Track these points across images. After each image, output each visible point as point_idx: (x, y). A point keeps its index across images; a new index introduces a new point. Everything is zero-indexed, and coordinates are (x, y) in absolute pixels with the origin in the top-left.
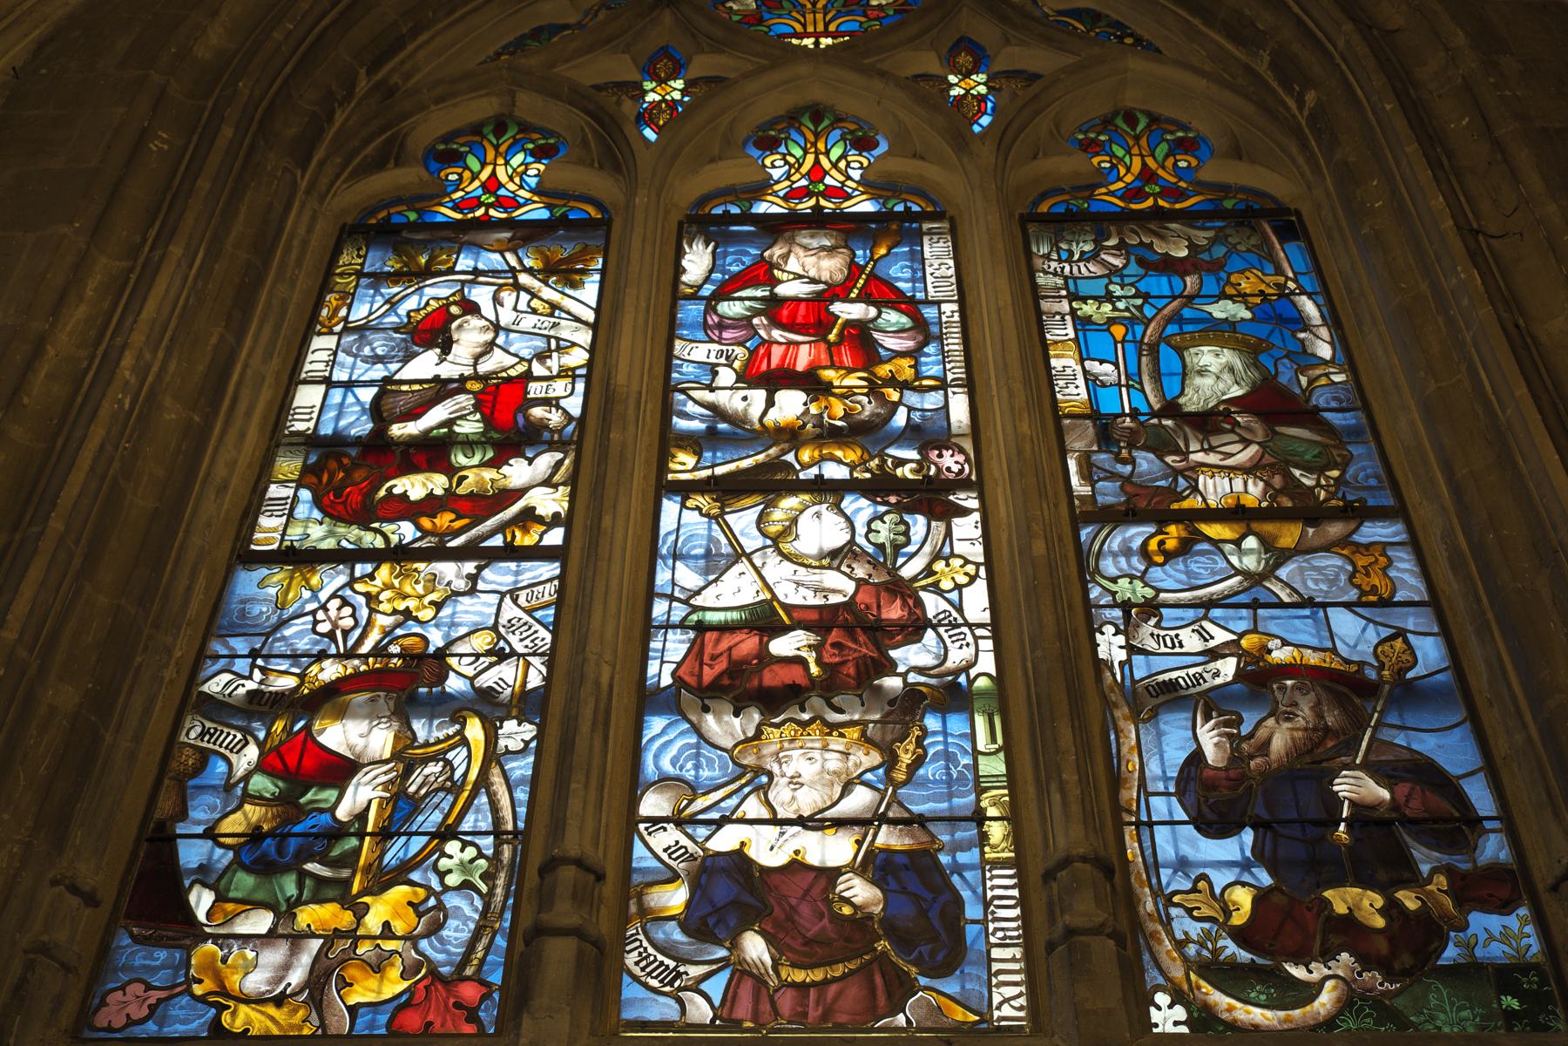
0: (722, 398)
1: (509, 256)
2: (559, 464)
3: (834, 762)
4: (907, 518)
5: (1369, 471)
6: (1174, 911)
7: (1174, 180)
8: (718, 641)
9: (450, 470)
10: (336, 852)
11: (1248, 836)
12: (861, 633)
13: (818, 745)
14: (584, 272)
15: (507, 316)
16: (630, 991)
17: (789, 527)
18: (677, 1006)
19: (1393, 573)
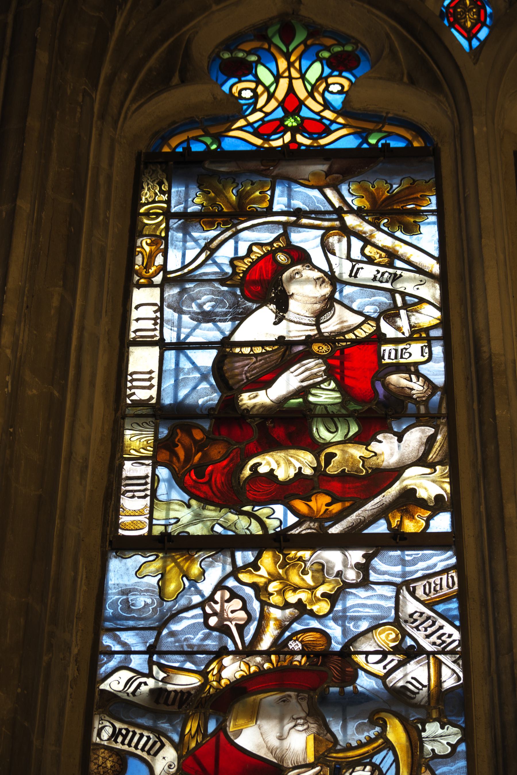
1: (329, 192)
2: (431, 441)
9: (315, 447)
14: (417, 213)
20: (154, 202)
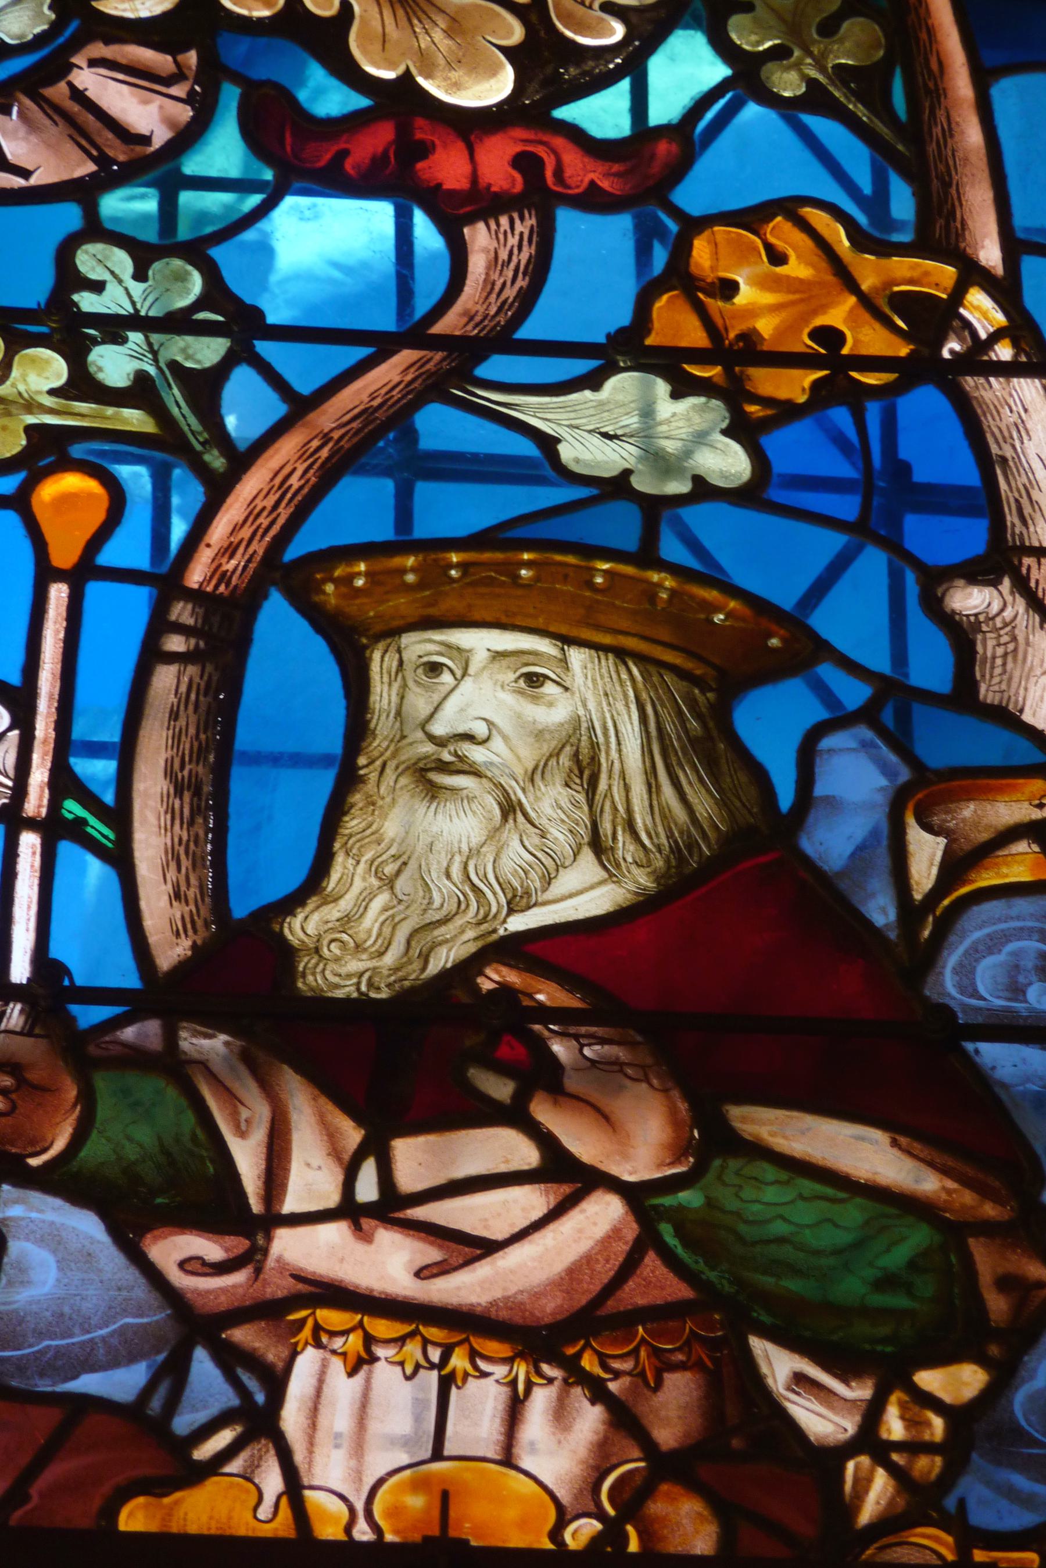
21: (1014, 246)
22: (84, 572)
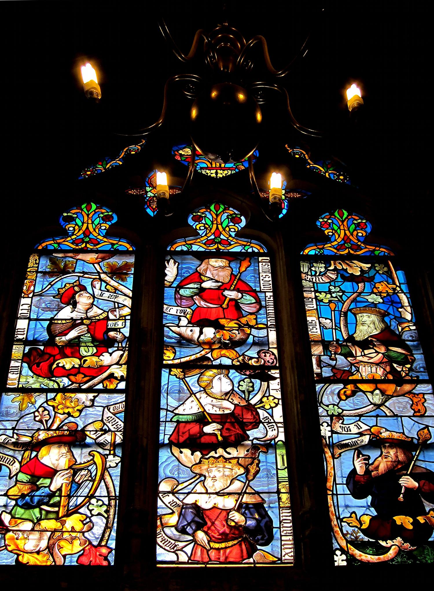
0: (183, 330)
2: (122, 356)
3: (227, 472)
4: (253, 380)
5: (421, 365)
6: (343, 524)
7: (356, 241)
8: (185, 427)
9: (81, 358)
10: (51, 502)
11: (370, 498)
12: (237, 425)
13: (222, 466)
14: (126, 274)
15: (97, 292)
16: (159, 550)
17: (210, 383)
18: (176, 556)
19: (425, 405)
20: (33, 267)
21: (400, 284)
22: (334, 311)
